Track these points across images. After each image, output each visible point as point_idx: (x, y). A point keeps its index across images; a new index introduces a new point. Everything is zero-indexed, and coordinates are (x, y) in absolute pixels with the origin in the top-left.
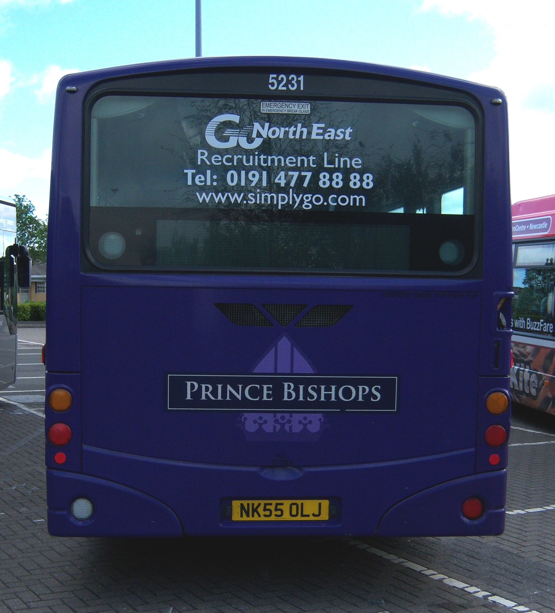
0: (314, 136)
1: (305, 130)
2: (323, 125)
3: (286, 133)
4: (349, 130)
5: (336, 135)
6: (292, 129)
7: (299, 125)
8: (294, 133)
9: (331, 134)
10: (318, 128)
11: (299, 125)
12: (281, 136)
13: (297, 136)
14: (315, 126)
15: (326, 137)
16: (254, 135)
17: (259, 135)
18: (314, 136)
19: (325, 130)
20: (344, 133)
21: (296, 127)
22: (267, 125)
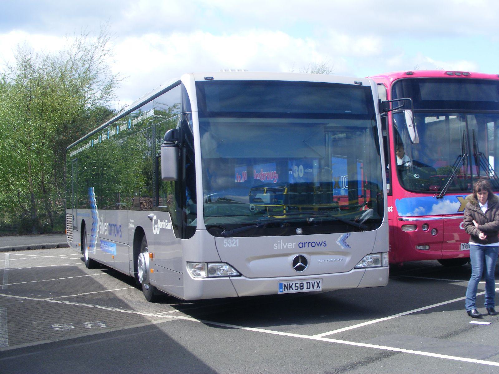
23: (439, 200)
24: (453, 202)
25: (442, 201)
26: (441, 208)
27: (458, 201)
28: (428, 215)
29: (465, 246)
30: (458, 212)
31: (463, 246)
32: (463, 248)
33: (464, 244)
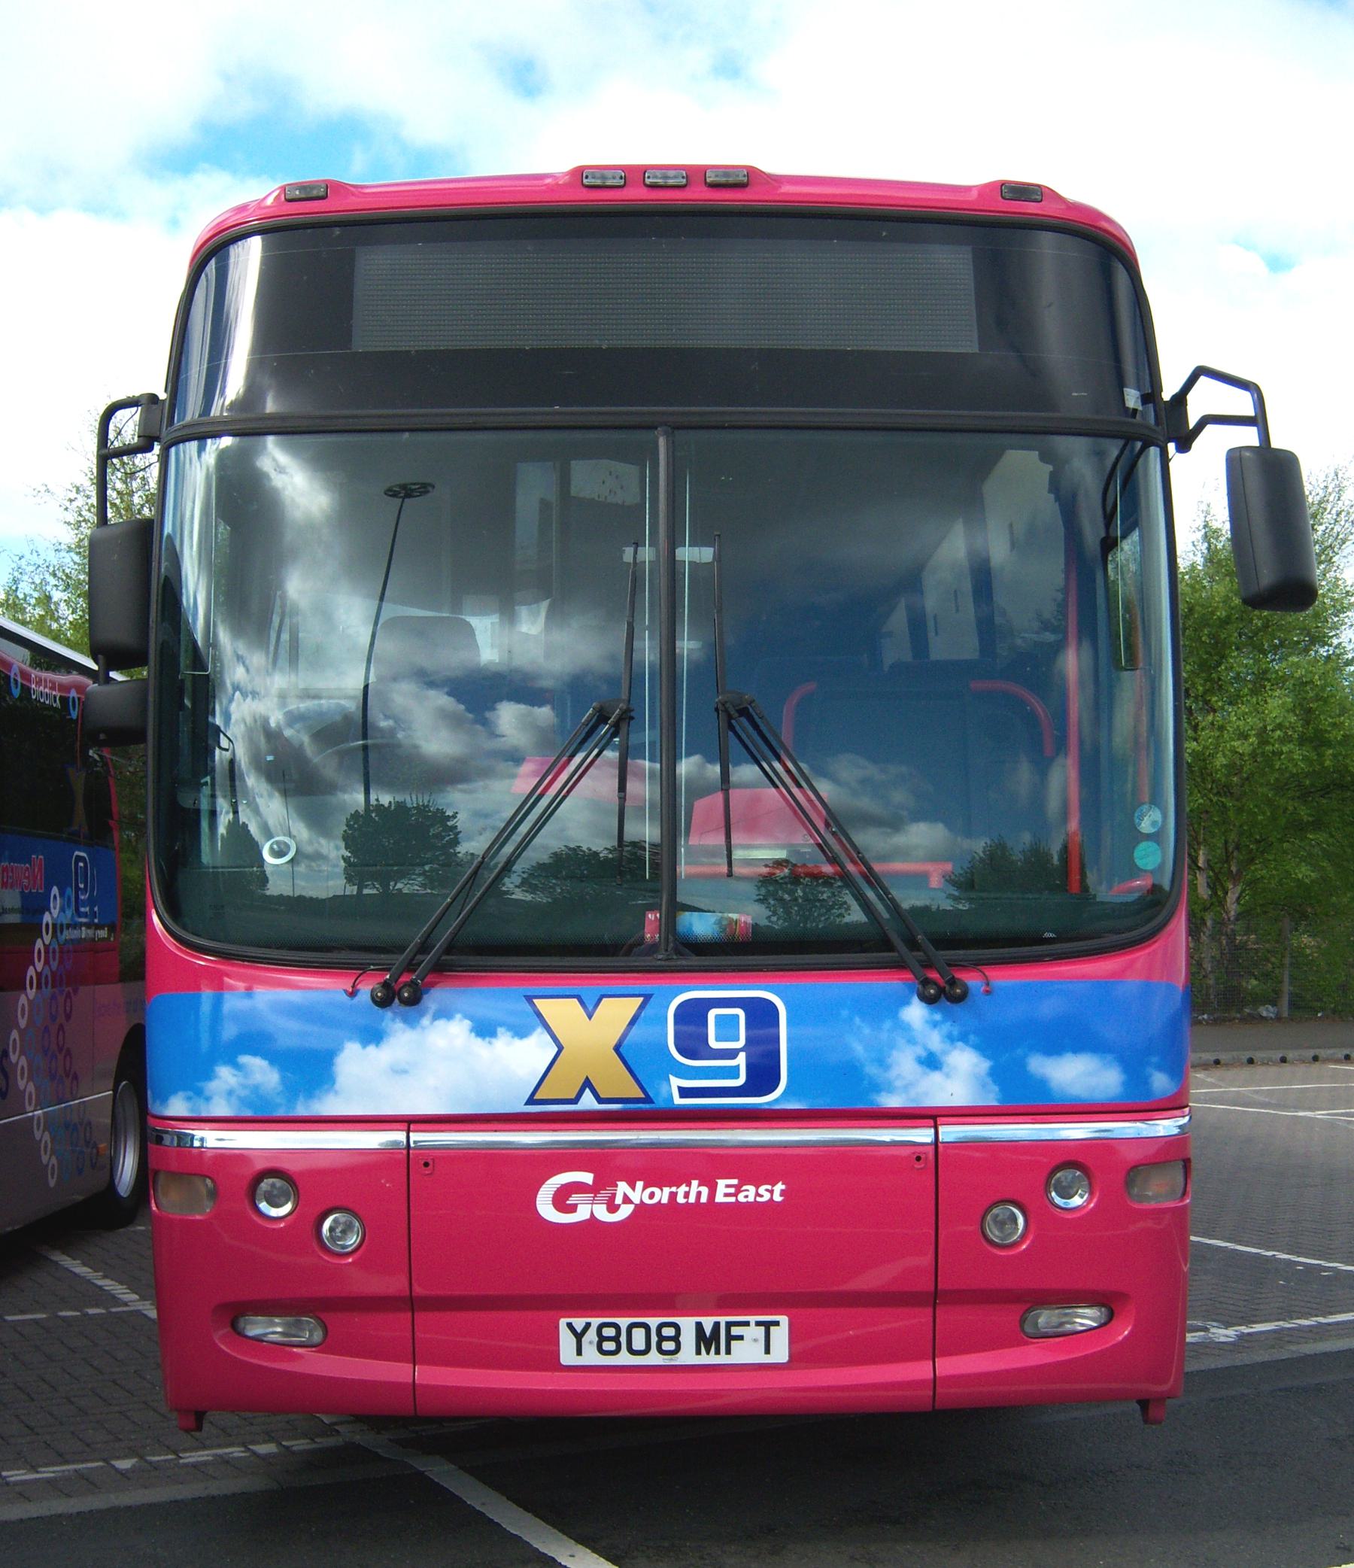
0: (720, 1198)
1: (705, 1190)
2: (735, 1182)
3: (673, 1196)
4: (780, 1187)
5: (758, 1194)
6: (683, 1188)
7: (695, 1183)
8: (687, 1195)
9: (748, 1194)
10: (728, 1186)
11: (695, 1183)
12: (665, 1200)
13: (692, 1199)
14: (722, 1183)
15: (741, 1198)
16: (618, 1200)
17: (627, 1200)
18: (720, 1198)
19: (738, 1189)
20: (771, 1192)
21: (689, 1185)
22: (640, 1184)
23: (391, 1020)
24: (500, 1030)
25: (411, 1022)
26: (399, 1071)
27: (540, 1030)
28: (301, 1111)
29: (591, 1335)
30: (531, 1101)
31: (579, 1336)
32: (579, 1352)
33: (588, 1325)
